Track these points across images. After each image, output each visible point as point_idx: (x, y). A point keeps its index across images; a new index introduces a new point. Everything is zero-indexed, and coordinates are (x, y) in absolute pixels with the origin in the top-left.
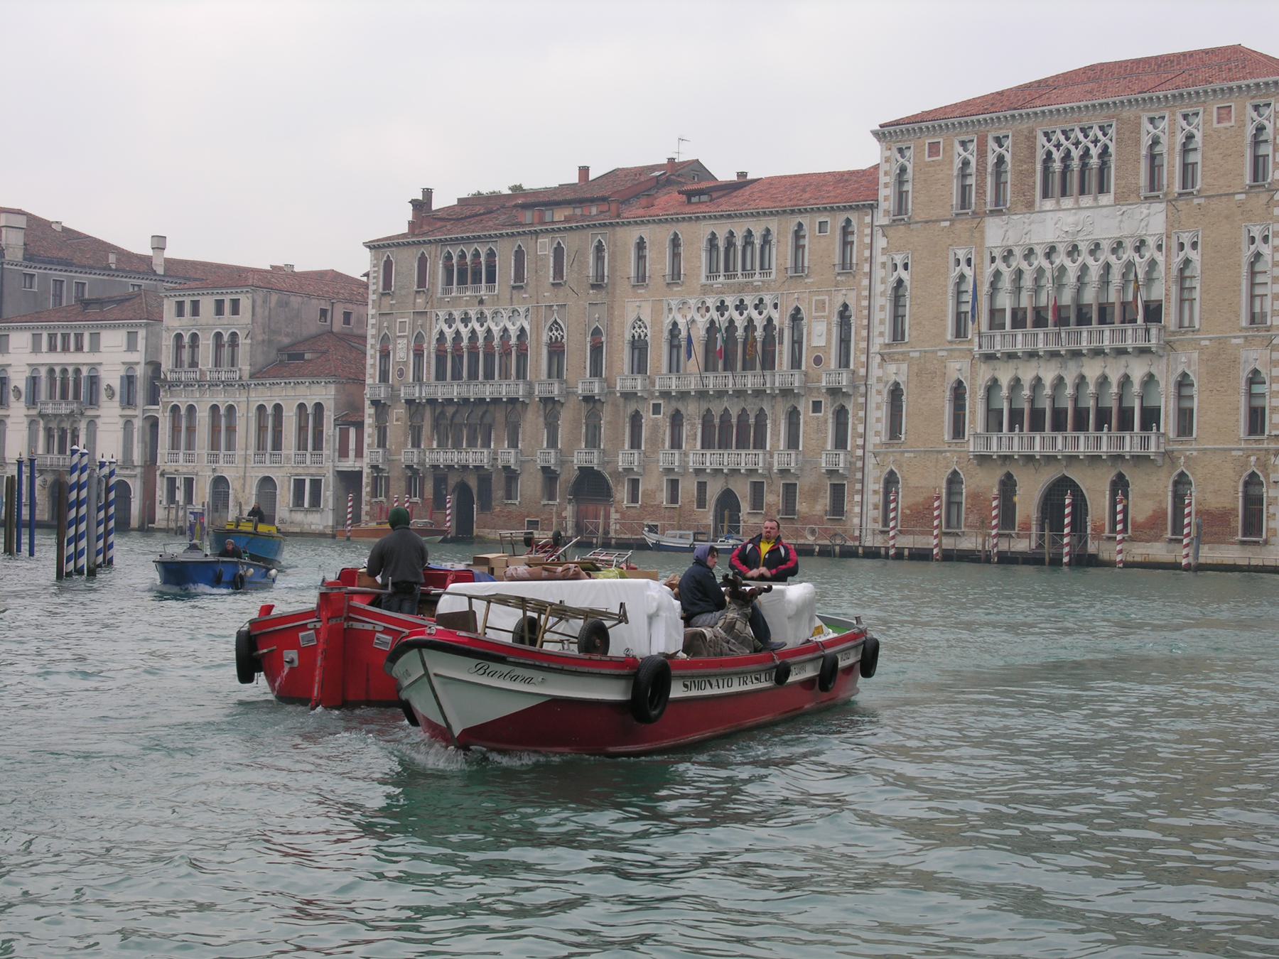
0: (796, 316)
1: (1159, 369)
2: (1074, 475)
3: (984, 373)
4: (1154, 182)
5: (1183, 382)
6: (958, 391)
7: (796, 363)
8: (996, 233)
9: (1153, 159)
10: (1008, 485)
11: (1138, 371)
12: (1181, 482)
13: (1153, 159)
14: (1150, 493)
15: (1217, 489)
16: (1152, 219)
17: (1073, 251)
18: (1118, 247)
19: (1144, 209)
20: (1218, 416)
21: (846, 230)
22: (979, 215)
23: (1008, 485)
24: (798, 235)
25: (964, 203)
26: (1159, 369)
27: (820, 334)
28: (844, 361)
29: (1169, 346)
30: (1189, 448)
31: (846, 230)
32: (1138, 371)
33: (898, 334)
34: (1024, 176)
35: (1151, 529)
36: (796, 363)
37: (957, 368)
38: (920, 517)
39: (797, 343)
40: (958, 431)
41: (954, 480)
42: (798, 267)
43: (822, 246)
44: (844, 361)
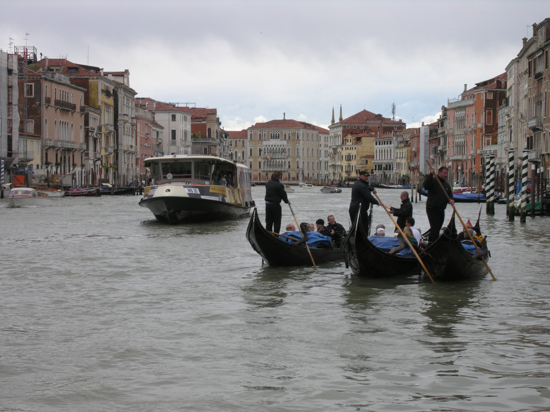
0: (236, 152)
1: (286, 160)
3: (263, 161)
4: (285, 138)
5: (289, 162)
6: (260, 163)
8: (265, 143)
9: (285, 135)
10: (267, 174)
11: (283, 161)
12: (289, 174)
13: (285, 135)
14: (285, 175)
15: (293, 175)
16: (285, 143)
17: (275, 146)
18: (281, 146)
19: (284, 141)
21: (243, 141)
22: (262, 141)
23: (267, 174)
24: (236, 141)
25: (260, 139)
26: (286, 160)
27: (240, 155)
29: (287, 158)
30: (290, 170)
31: (243, 141)
33: (251, 154)
34: (268, 136)
37: (260, 160)
38: (256, 178)
39: (236, 156)
40: (260, 167)
41: (260, 174)
43: (240, 144)
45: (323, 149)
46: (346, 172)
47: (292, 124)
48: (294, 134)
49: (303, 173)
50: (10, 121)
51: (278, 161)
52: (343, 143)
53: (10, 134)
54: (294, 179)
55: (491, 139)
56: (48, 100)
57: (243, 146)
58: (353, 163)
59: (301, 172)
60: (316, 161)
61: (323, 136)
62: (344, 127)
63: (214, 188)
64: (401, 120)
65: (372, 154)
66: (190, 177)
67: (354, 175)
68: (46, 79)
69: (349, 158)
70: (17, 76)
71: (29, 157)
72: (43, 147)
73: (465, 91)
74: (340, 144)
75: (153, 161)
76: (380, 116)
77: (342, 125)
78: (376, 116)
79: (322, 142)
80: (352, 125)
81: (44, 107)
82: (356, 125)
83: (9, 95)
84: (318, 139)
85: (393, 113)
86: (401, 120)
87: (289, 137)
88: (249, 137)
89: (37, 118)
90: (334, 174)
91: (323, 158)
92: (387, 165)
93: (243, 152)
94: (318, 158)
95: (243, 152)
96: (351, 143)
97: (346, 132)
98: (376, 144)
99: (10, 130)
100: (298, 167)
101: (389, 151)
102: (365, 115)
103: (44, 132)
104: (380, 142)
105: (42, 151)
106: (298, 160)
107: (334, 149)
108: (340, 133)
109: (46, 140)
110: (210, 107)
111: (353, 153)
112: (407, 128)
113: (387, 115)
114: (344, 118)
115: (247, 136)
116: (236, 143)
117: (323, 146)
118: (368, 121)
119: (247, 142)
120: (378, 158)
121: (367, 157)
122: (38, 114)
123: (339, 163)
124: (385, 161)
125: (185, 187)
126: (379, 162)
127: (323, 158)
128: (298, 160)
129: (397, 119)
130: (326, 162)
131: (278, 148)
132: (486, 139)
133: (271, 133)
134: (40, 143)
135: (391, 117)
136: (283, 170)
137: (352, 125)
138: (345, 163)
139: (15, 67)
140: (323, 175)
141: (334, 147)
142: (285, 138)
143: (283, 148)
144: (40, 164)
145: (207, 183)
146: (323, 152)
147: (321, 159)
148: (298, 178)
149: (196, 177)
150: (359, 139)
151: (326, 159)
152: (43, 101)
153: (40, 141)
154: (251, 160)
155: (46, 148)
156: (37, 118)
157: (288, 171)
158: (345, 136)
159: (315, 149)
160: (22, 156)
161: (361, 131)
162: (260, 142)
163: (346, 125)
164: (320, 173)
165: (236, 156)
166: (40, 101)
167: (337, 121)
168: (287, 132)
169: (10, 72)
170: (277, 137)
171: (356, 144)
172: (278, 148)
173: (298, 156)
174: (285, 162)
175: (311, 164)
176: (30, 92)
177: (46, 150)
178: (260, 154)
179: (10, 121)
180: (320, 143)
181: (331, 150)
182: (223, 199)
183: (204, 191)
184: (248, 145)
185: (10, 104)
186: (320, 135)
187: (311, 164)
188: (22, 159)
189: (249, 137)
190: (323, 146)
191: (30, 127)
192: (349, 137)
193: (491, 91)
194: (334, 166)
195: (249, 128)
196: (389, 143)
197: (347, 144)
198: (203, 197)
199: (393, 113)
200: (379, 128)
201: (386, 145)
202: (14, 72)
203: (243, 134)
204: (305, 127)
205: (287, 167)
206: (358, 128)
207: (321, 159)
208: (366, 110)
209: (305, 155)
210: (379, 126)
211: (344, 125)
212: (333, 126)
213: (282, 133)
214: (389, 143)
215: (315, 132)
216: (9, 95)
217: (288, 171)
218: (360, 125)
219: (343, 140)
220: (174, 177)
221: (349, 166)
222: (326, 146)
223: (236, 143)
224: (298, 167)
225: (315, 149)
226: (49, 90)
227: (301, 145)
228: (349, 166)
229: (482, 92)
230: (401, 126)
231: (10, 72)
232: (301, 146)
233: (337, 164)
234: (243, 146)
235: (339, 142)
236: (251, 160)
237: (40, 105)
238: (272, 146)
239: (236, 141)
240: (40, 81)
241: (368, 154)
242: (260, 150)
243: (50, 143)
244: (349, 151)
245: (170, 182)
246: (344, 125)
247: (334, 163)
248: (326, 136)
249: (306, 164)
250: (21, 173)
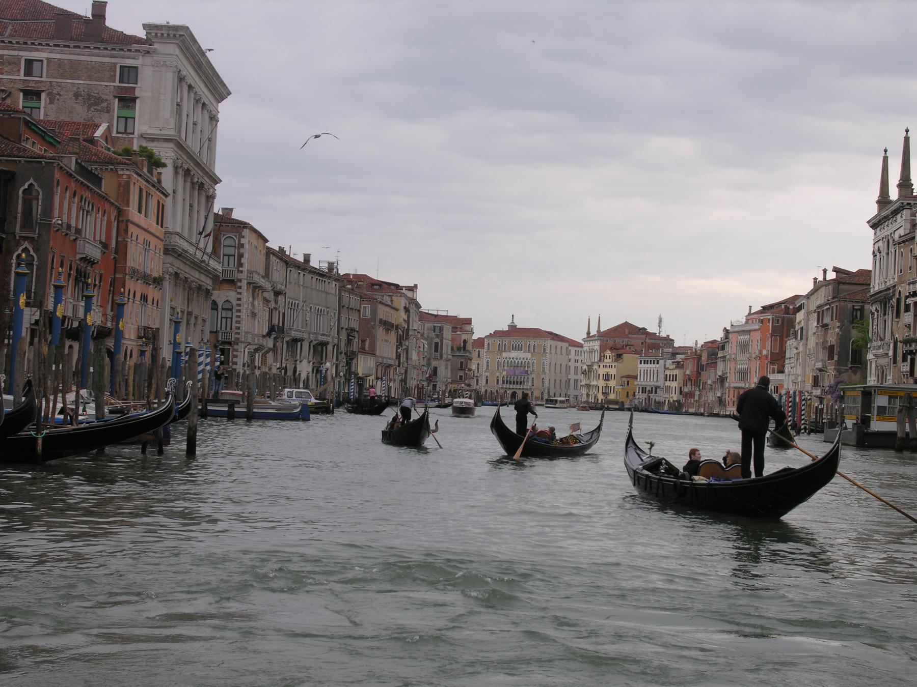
8: (504, 355)
16: (529, 355)
37: (498, 374)
45: (572, 365)
52: (600, 360)
58: (612, 383)
61: (573, 349)
65: (633, 374)
67: (612, 396)
69: (607, 377)
73: (750, 314)
76: (644, 329)
78: (640, 329)
84: (568, 353)
85: (660, 326)
88: (486, 346)
90: (588, 395)
91: (572, 376)
97: (603, 349)
102: (626, 330)
110: (462, 316)
111: (613, 371)
113: (652, 329)
119: (483, 352)
121: (628, 377)
123: (595, 383)
128: (543, 376)
129: (663, 335)
130: (576, 381)
135: (657, 332)
138: (602, 383)
146: (572, 368)
150: (619, 357)
151: (576, 377)
154: (487, 374)
167: (593, 332)
170: (520, 348)
171: (616, 361)
175: (558, 382)
181: (585, 367)
186: (570, 348)
187: (558, 382)
192: (608, 353)
194: (588, 386)
205: (530, 384)
213: (525, 344)
215: (565, 345)
221: (607, 386)
228: (607, 386)
230: (668, 341)
236: (487, 374)
243: (380, 360)
244: (607, 370)
247: (588, 382)
248: (577, 349)
249: (552, 381)
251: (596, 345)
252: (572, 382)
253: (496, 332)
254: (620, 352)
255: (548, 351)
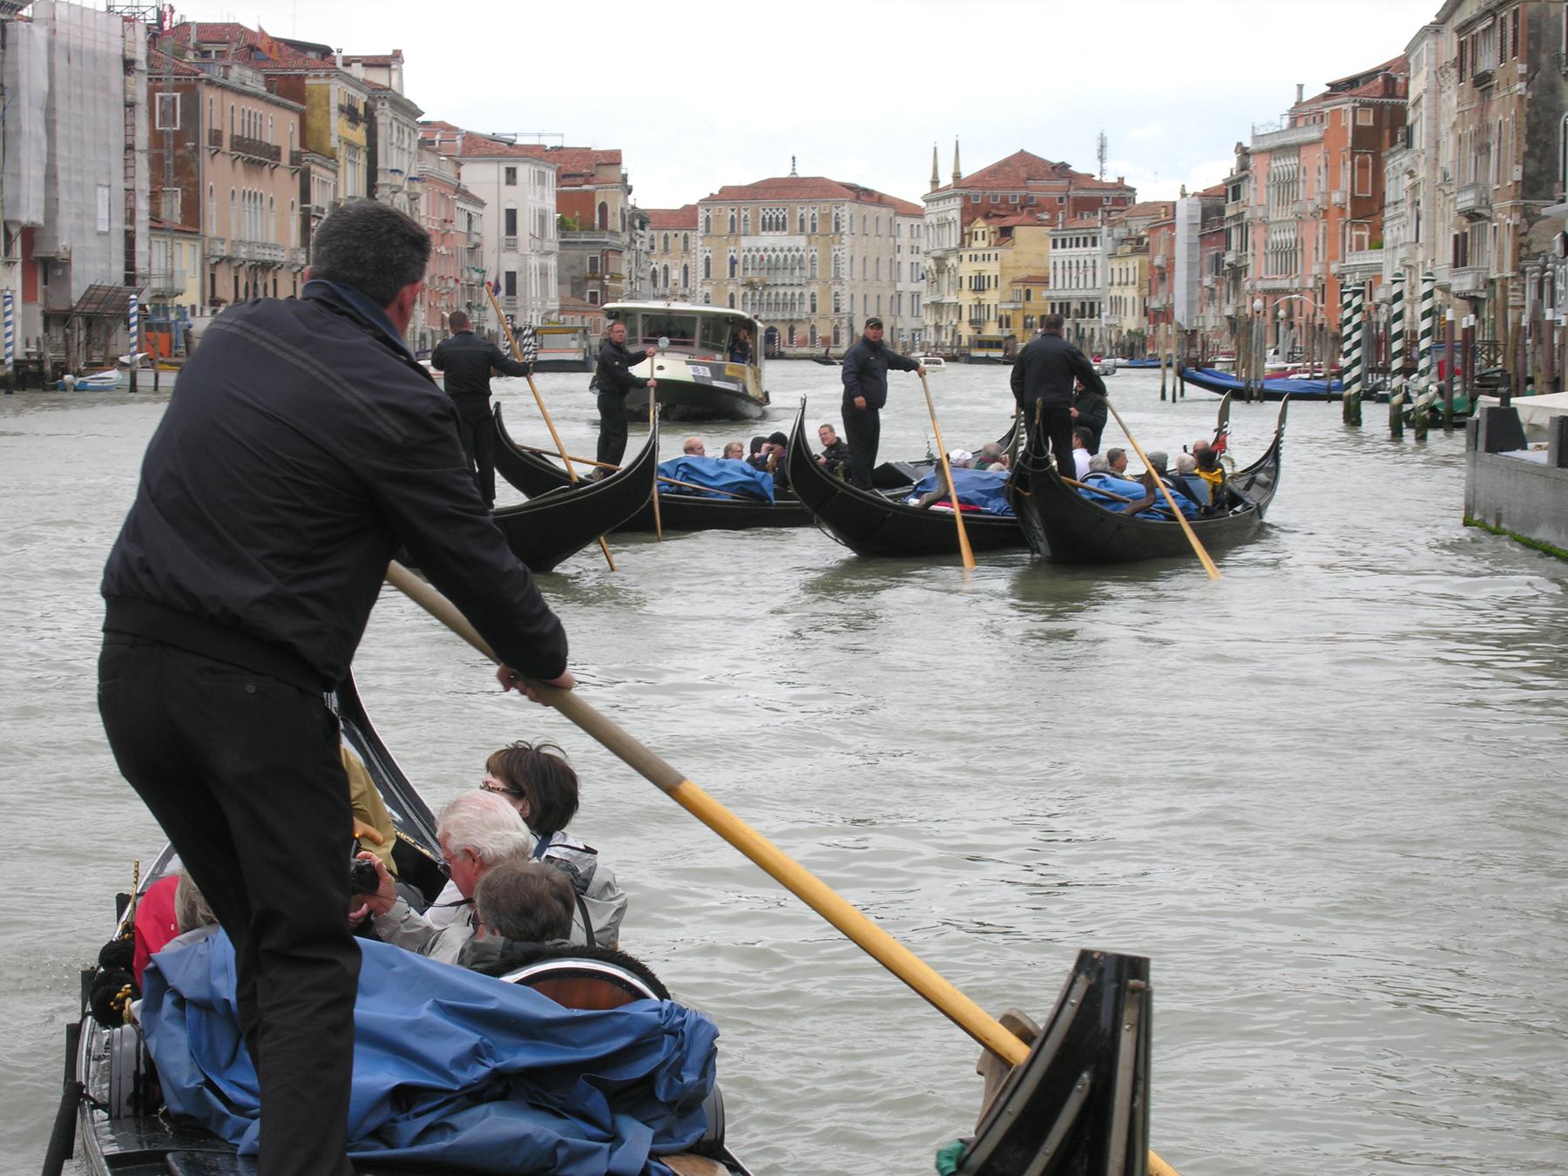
0: (666, 268)
1: (805, 291)
2: (776, 325)
4: (802, 229)
5: (813, 295)
7: (666, 285)
8: (745, 242)
9: (802, 221)
11: (797, 291)
12: (813, 327)
13: (802, 221)
14: (802, 331)
15: (824, 330)
16: (801, 241)
20: (825, 306)
21: (686, 237)
24: (666, 237)
25: (732, 230)
26: (805, 291)
27: (676, 274)
28: (686, 285)
29: (808, 283)
30: (815, 317)
31: (686, 237)
32: (797, 291)
33: (708, 275)
35: (803, 343)
36: (666, 285)
37: (731, 289)
39: (666, 278)
42: (666, 250)
43: (676, 244)
44: (686, 285)
45: (905, 259)
46: (971, 322)
47: (817, 189)
48: (825, 217)
49: (851, 327)
50: (130, 193)
51: (781, 291)
52: (963, 242)
53: (129, 227)
54: (825, 341)
55: (1366, 234)
56: (216, 137)
57: (686, 249)
58: (991, 297)
59: (845, 322)
60: (889, 293)
61: (905, 224)
62: (966, 198)
63: (730, 368)
64: (1121, 180)
65: (1040, 273)
66: (692, 344)
67: (992, 330)
68: (210, 83)
69: (979, 284)
70: (145, 78)
71: (177, 286)
72: (205, 258)
73: (1299, 104)
74: (953, 245)
75: (623, 309)
77: (959, 191)
78: (1055, 167)
79: (904, 240)
80: (988, 192)
81: (205, 155)
82: (1000, 193)
83: (129, 126)
84: (894, 232)
85: (1101, 158)
86: (1121, 180)
87: (814, 226)
88: (701, 224)
89: (189, 184)
90: (938, 328)
91: (906, 285)
92: (1083, 304)
93: (686, 268)
94: (893, 283)
95: (686, 268)
96: (984, 244)
97: (970, 213)
98: (1055, 246)
99: (131, 218)
100: (837, 310)
101: (1090, 264)
102: (1024, 166)
103: (207, 221)
104: (1064, 241)
105: (203, 269)
106: (836, 288)
107: (936, 259)
108: (955, 215)
109: (213, 240)
111: (991, 269)
112: (1139, 200)
113: (1083, 164)
114: (966, 173)
115: (695, 222)
116: (666, 243)
117: (905, 250)
118: (1031, 183)
119: (697, 239)
120: (1059, 286)
122: (191, 173)
123: (950, 298)
124: (1079, 293)
125: (688, 363)
126: (1063, 294)
127: (906, 285)
128: (836, 288)
129: (1110, 178)
130: (916, 296)
131: (782, 256)
132: (1355, 233)
133: (762, 213)
134: (199, 250)
136: (795, 316)
137: (988, 192)
138: (967, 299)
139: (140, 54)
140: (907, 332)
141: (938, 254)
142: (802, 229)
143: (797, 255)
144: (198, 304)
145: (719, 356)
146: (905, 268)
147: (900, 287)
148: (837, 340)
149: (703, 346)
150: (1006, 232)
151: (915, 287)
152: (205, 140)
153: (199, 245)
154: (708, 289)
155: (213, 261)
156: (189, 184)
157: (809, 319)
158: (969, 223)
159: (885, 259)
160: (157, 284)
161: (1013, 210)
162: (732, 239)
163: (972, 192)
164: (899, 326)
165: (666, 278)
166: (197, 140)
167: (946, 180)
168: (807, 211)
169: (129, 65)
170: (779, 226)
171: (998, 244)
172: (782, 256)
173: (838, 279)
174: (801, 294)
176: (168, 118)
177: (212, 266)
178: (732, 274)
179: (130, 193)
180: (899, 241)
182: (745, 388)
183: (717, 372)
184: (700, 248)
185: (130, 148)
186: (899, 220)
188: (158, 290)
189: (701, 224)
190: (905, 250)
191: (173, 209)
192: (980, 225)
193: (1369, 105)
194: (938, 306)
195: (703, 202)
196: (1089, 242)
197: (975, 244)
198: (716, 384)
199: (1101, 158)
200: (1061, 200)
201: (1081, 248)
202: (138, 66)
203: (685, 218)
204: (858, 197)
205: (807, 307)
206: (1005, 200)
207: (900, 287)
208: (1027, 150)
209: (858, 275)
210: (1062, 194)
211: (965, 192)
212: (937, 194)
213: (793, 214)
214: (1089, 242)
215: (884, 212)
216: (129, 126)
217: (809, 319)
218: (1011, 193)
219: (963, 235)
220: (672, 343)
221: (979, 306)
222: (915, 250)
223: (666, 243)
224: (837, 310)
225: (885, 259)
226: (219, 111)
227: (845, 248)
228: (979, 306)
229: (1344, 107)
231: (129, 65)
232: (847, 250)
233: (946, 300)
234: (686, 249)
235: (952, 238)
237: (196, 149)
238: (766, 250)
239: (666, 237)
240: (194, 87)
241: (1032, 273)
242: (733, 262)
243: (223, 250)
244: (979, 266)
245: (663, 352)
246: (965, 192)
247: (936, 298)
248: (915, 222)
250: (160, 326)
251: (953, 210)
252: (906, 302)
253: (726, 191)
254: (1008, 222)
255: (845, 228)
